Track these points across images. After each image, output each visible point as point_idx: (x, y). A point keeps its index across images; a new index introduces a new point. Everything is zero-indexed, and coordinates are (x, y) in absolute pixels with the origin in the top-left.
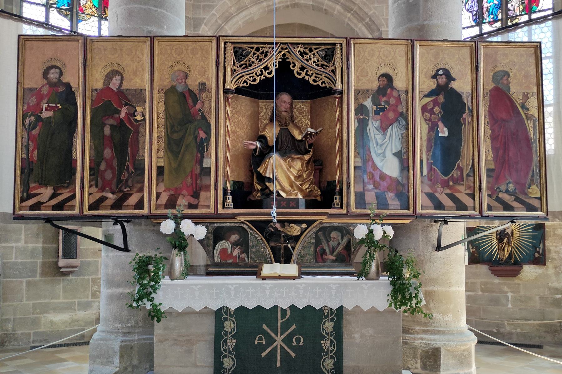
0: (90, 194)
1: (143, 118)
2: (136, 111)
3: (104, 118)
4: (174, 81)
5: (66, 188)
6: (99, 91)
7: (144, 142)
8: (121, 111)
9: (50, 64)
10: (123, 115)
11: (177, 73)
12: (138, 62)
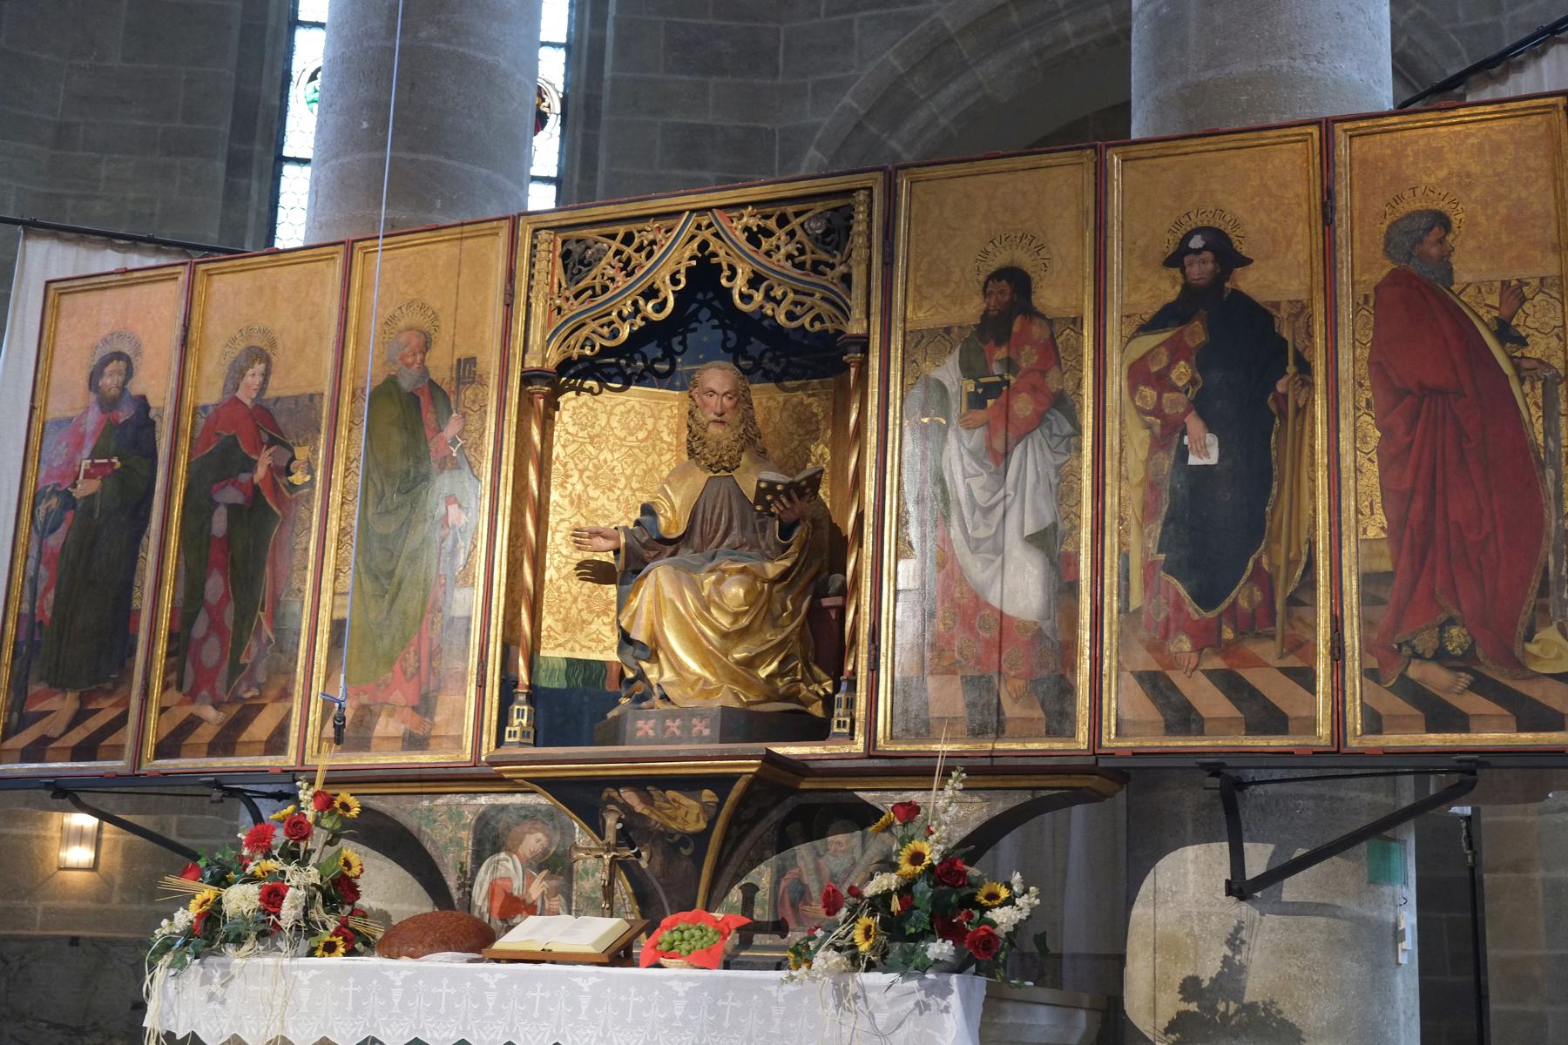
0: (163, 710)
1: (308, 478)
2: (293, 458)
3: (215, 487)
4: (395, 363)
5: (109, 694)
6: (211, 410)
7: (306, 549)
8: (256, 461)
9: (108, 349)
10: (261, 472)
11: (403, 338)
12: (311, 319)
